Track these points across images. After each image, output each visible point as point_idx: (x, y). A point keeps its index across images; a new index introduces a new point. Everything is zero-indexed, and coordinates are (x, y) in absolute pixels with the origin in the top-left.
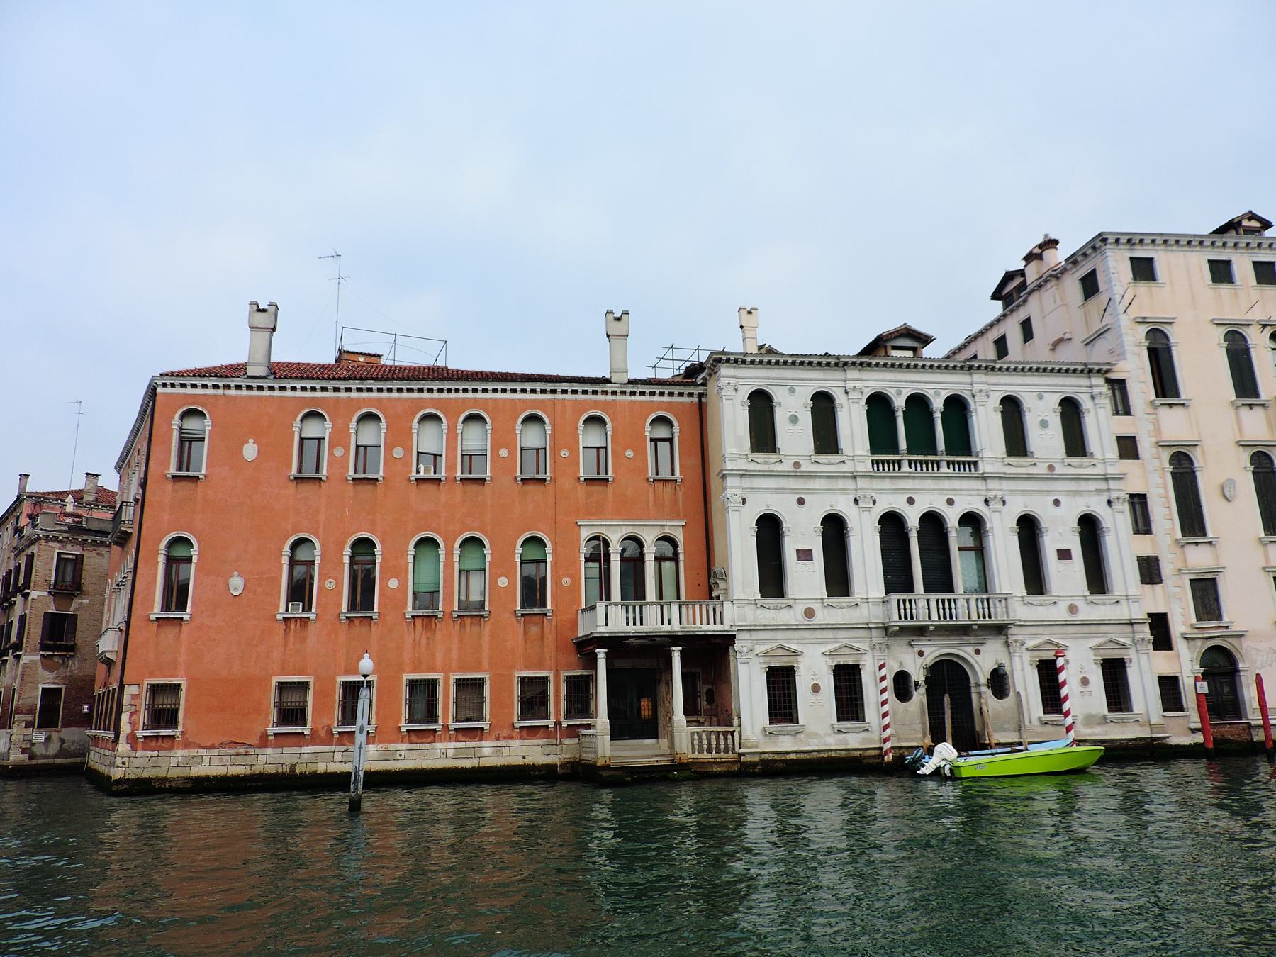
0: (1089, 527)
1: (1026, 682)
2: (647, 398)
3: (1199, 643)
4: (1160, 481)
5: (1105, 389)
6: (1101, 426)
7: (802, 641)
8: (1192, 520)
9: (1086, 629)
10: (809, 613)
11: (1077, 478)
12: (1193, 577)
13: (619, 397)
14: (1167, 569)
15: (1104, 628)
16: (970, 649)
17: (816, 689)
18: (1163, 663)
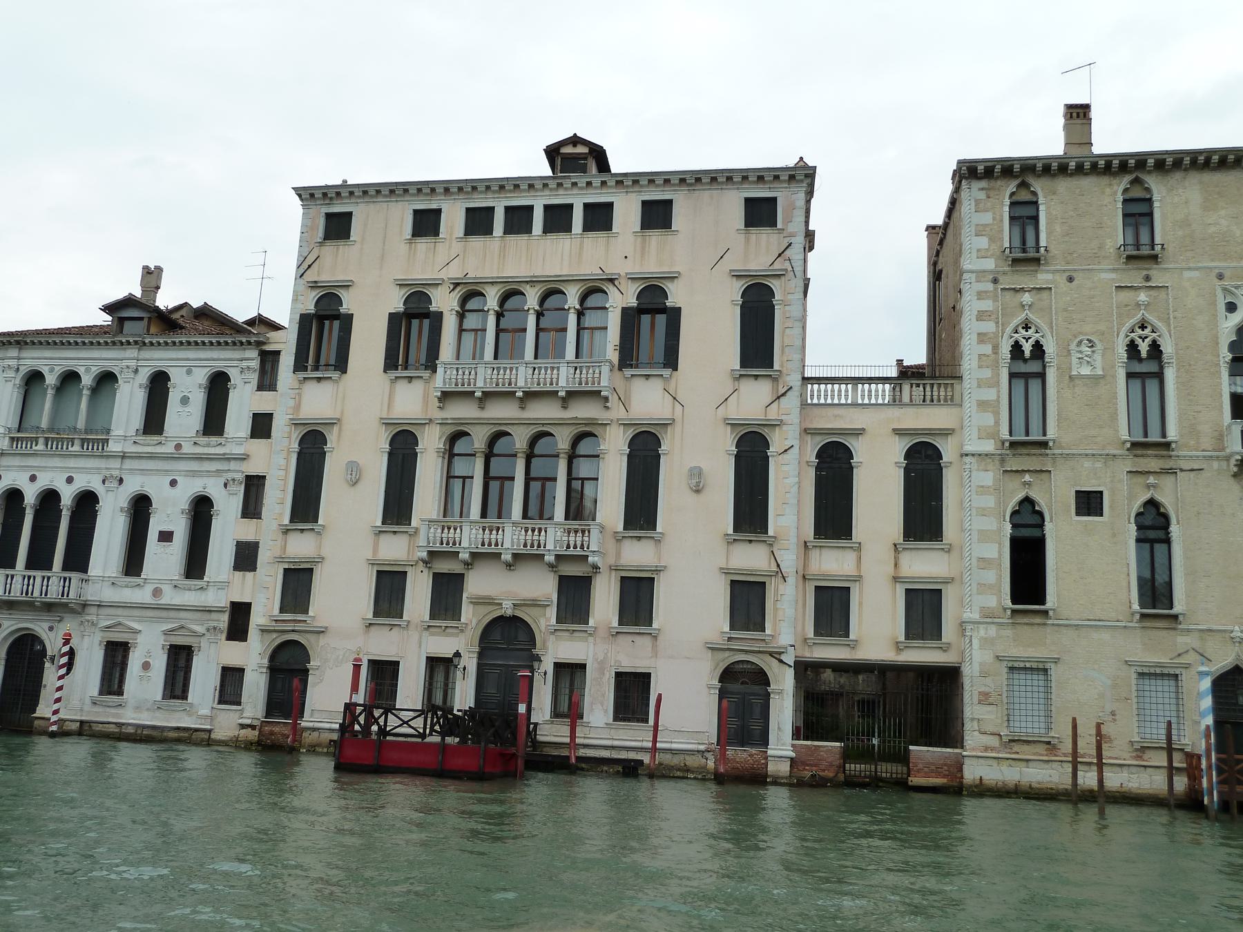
0: (201, 510)
1: (91, 661)
4: (283, 462)
5: (255, 364)
6: (244, 401)
8: (306, 506)
9: (164, 614)
14: (263, 556)
15: (183, 614)
16: (46, 625)
18: (233, 653)
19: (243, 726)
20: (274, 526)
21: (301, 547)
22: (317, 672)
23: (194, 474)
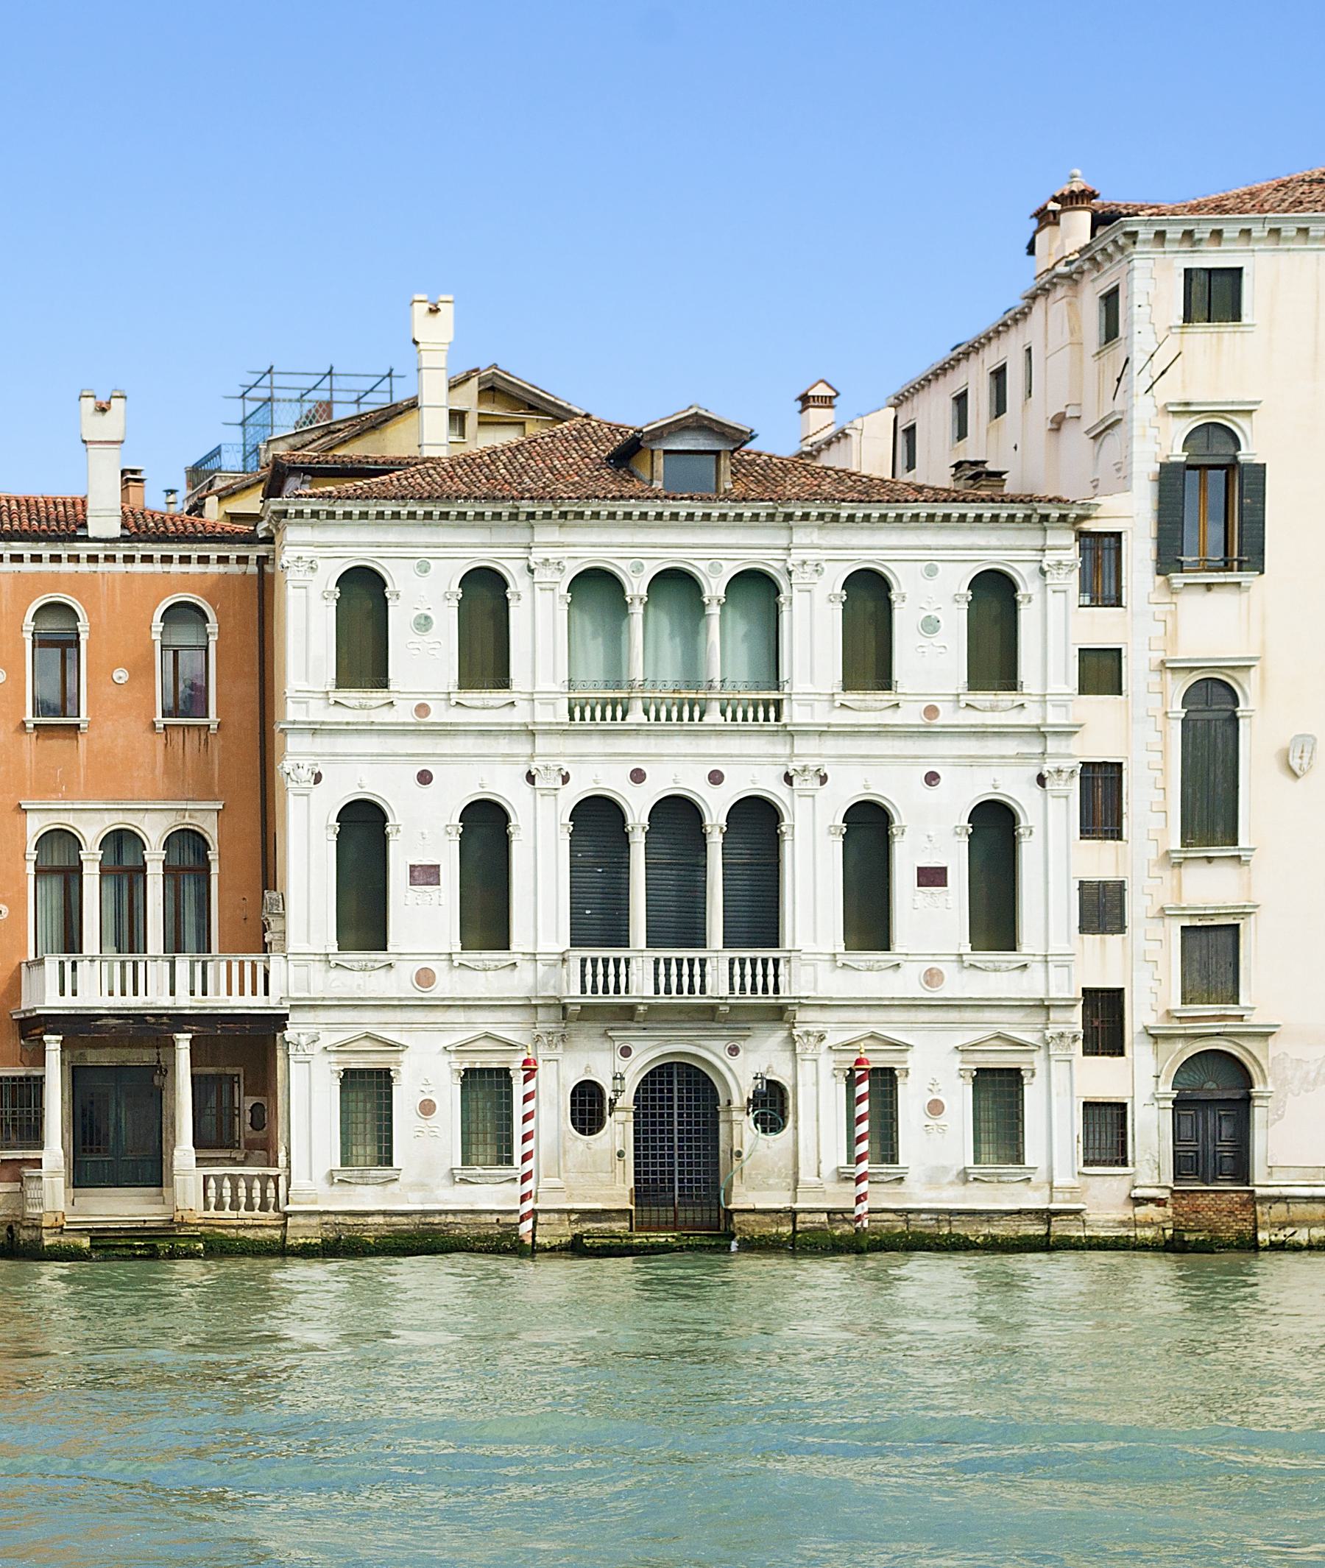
2: (158, 567)
3: (1179, 1045)
7: (408, 1026)
8: (1211, 812)
9: (953, 1015)
10: (425, 978)
11: (980, 733)
12: (1187, 923)
13: (102, 567)
14: (1135, 907)
16: (720, 1047)
17: (427, 1108)
18: (1103, 1078)
19: (1138, 1201)
20: (1153, 853)
21: (1210, 887)
22: (1269, 1103)
23: (974, 761)
